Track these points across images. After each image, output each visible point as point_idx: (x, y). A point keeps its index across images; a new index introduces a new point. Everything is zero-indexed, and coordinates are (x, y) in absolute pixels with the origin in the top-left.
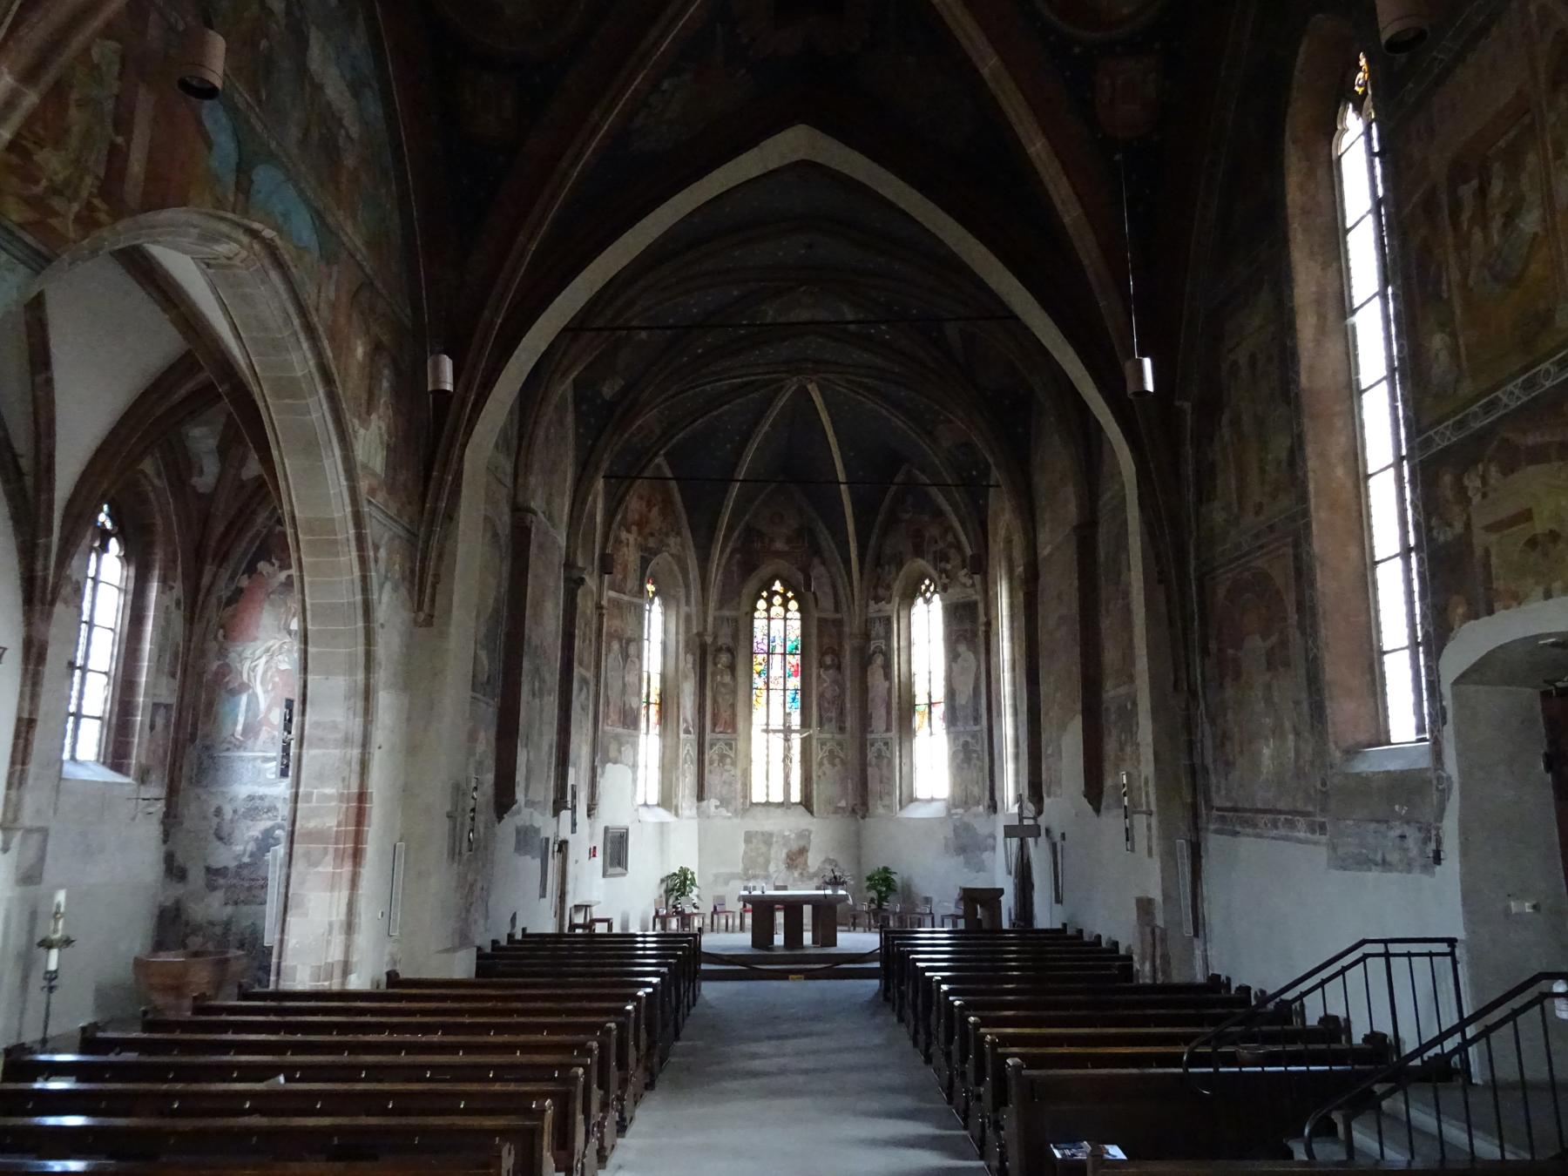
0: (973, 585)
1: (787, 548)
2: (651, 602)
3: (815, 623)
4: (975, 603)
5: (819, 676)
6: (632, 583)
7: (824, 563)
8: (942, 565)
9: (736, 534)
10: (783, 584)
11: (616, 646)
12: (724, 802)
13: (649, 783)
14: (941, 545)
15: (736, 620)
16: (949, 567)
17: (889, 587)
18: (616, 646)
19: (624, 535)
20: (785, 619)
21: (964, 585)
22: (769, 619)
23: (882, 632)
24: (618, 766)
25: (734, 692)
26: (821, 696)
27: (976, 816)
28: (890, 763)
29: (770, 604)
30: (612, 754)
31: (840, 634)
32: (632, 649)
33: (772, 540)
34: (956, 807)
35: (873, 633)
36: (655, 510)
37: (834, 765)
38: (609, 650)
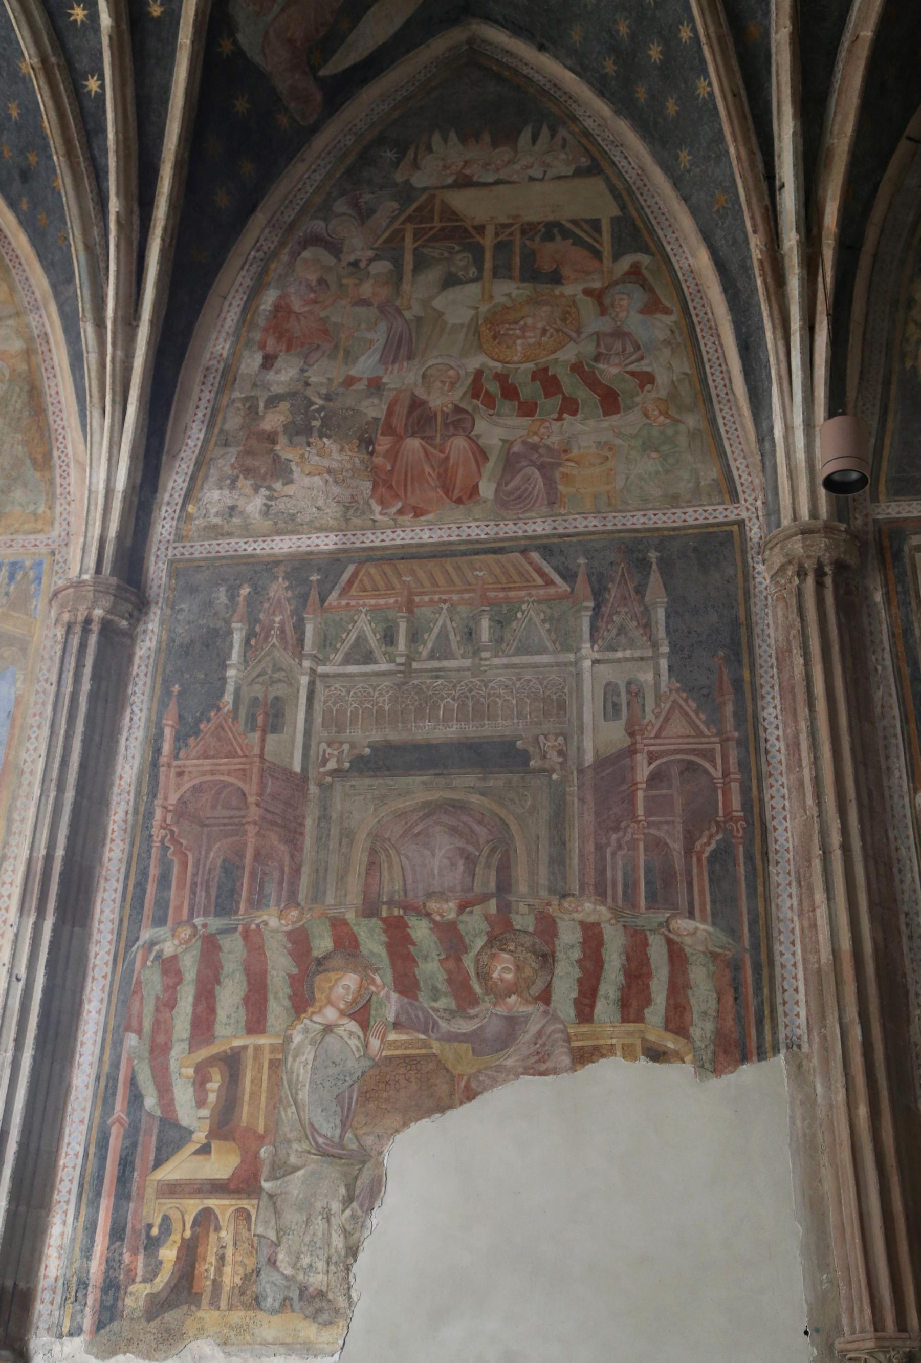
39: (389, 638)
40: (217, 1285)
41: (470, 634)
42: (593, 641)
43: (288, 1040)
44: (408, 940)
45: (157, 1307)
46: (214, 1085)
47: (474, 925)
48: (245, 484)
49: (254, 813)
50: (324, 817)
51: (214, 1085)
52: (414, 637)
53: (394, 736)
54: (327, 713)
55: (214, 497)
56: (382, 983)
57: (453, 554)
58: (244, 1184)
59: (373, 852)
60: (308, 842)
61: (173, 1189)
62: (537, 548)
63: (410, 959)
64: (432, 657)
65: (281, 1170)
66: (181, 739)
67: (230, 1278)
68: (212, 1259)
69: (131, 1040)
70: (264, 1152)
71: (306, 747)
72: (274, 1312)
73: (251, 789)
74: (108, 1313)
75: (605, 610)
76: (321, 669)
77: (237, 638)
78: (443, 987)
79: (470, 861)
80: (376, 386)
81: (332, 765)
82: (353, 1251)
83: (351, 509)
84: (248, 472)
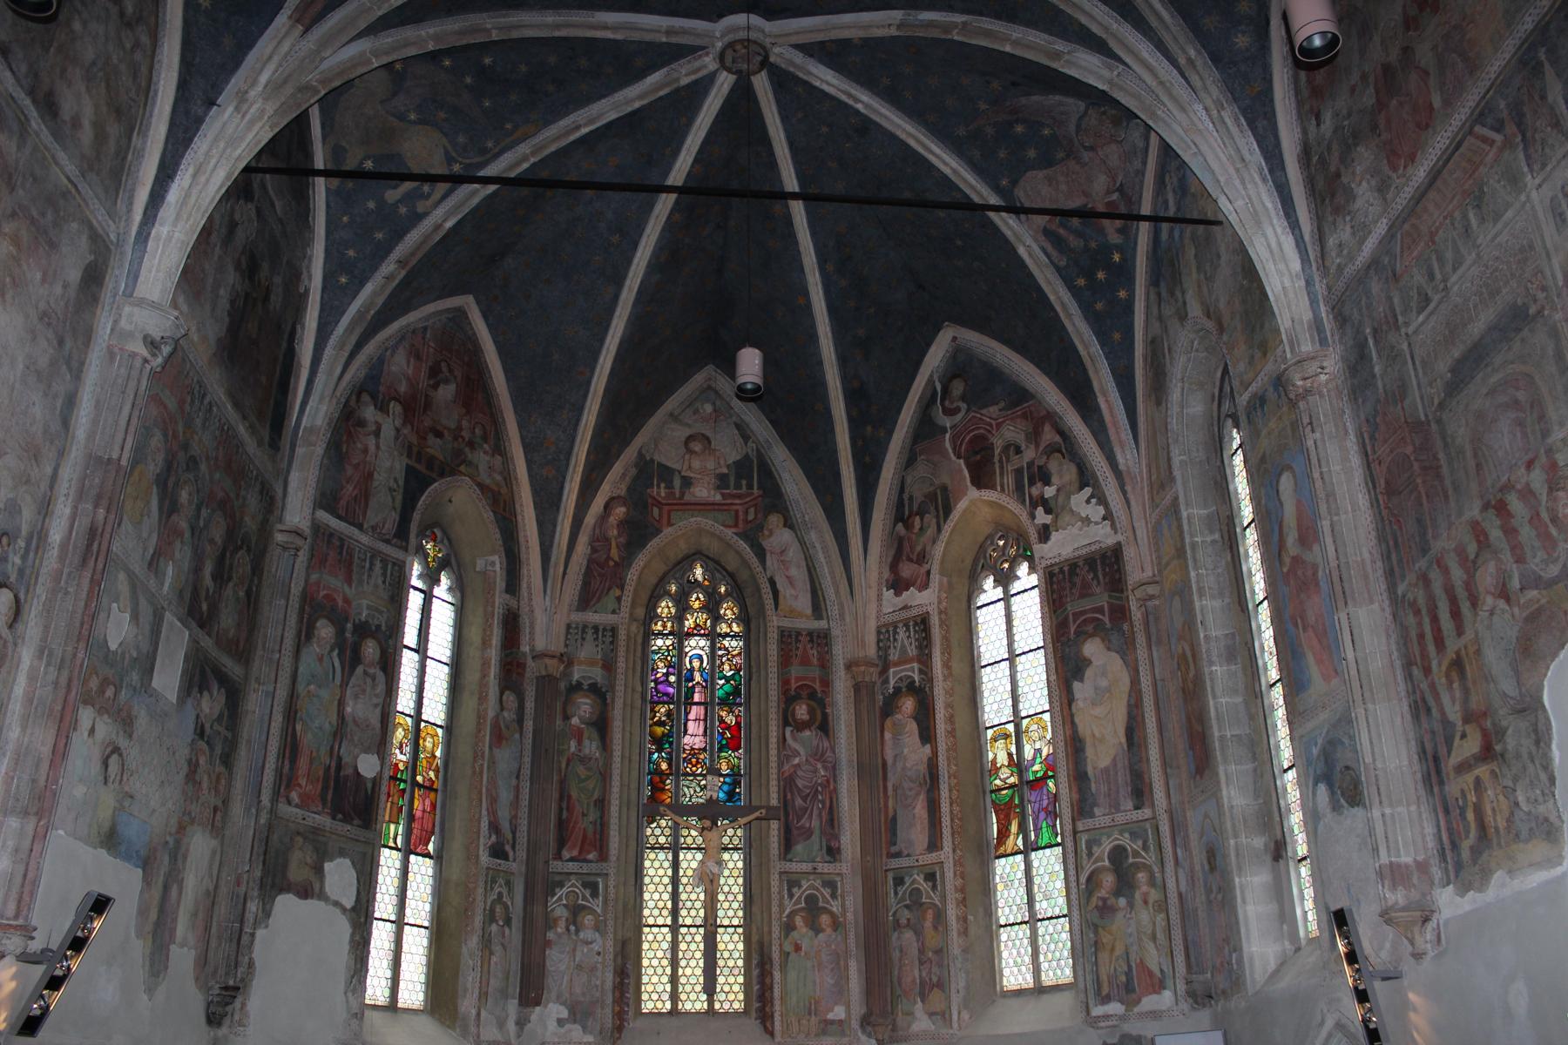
0: (1108, 516)
1: (718, 498)
2: (432, 579)
3: (773, 636)
4: (1117, 551)
5: (783, 740)
6: (382, 510)
7: (789, 524)
8: (1035, 491)
9: (618, 468)
10: (706, 569)
11: (325, 630)
12: (579, 1013)
13: (400, 966)
14: (1029, 454)
15: (614, 630)
16: (1049, 492)
17: (922, 558)
18: (325, 630)
19: (369, 413)
20: (713, 637)
21: (1087, 521)
22: (681, 636)
23: (912, 651)
24: (312, 905)
25: (605, 777)
26: (788, 783)
27: (1155, 1015)
28: (940, 916)
29: (683, 608)
30: (296, 873)
31: (825, 664)
32: (370, 649)
33: (687, 482)
34: (1106, 1000)
35: (894, 655)
36: (446, 392)
37: (817, 930)
38: (306, 634)
39: (1431, 277)
40: (1497, 829)
41: (1467, 229)
42: (1531, 171)
43: (1477, 633)
44: (1510, 515)
45: (1476, 852)
46: (1456, 685)
47: (1537, 479)
48: (1339, 219)
49: (1416, 466)
50: (1446, 445)
51: (1456, 685)
52: (1440, 259)
53: (1456, 354)
54: (1423, 362)
55: (1331, 242)
56: (1507, 556)
57: (1439, 172)
58: (1488, 753)
59: (1475, 455)
60: (1445, 470)
61: (1463, 768)
62: (1476, 122)
63: (1515, 531)
64: (1455, 270)
65: (1501, 733)
66: (1372, 438)
67: (1502, 824)
68: (1489, 812)
69: (1416, 671)
70: (1489, 724)
71: (1422, 398)
72: (1527, 841)
73: (1409, 450)
74: (1459, 866)
75: (1529, 134)
76: (1410, 330)
77: (1371, 341)
78: (1537, 544)
79: (1521, 423)
80: (1364, 77)
81: (1436, 402)
82: (1552, 780)
83: (1382, 188)
84: (1337, 210)
